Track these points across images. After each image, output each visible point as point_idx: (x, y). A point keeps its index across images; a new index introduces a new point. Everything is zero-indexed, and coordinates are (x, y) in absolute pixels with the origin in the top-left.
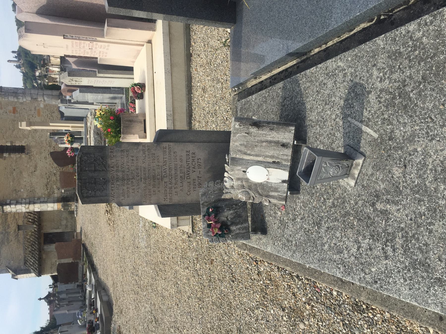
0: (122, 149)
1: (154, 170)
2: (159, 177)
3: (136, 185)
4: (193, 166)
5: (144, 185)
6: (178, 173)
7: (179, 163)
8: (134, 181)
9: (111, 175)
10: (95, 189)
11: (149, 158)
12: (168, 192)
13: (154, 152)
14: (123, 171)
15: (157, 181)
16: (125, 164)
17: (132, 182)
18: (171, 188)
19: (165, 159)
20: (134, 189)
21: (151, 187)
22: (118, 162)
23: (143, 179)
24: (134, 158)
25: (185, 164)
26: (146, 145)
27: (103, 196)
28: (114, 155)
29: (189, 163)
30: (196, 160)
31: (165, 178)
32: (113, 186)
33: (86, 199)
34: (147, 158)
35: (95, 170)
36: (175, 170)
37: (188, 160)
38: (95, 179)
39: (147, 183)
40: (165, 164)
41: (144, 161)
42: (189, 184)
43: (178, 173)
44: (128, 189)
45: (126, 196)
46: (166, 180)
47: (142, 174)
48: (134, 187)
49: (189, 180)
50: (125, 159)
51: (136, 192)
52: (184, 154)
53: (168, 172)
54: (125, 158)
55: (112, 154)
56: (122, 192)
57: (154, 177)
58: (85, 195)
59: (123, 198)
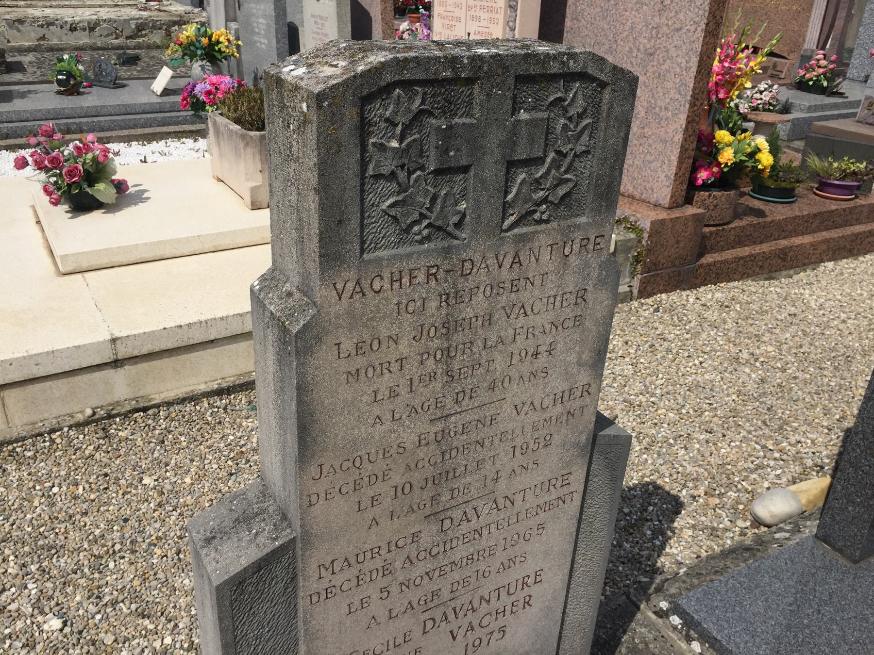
0: (589, 297)
1: (480, 463)
2: (445, 497)
3: (417, 402)
4: (475, 623)
5: (409, 438)
6: (456, 576)
7: (501, 556)
8: (437, 385)
9: (477, 258)
10: (410, 173)
11: (535, 429)
12: (369, 565)
13: (557, 439)
14: (489, 320)
15: (427, 494)
16: (522, 320)
17: (433, 377)
18: (386, 570)
19: (519, 498)
20: (393, 394)
21: (397, 479)
22: (538, 282)
23: (440, 426)
24: (543, 358)
25: (487, 588)
26: (588, 400)
27: (362, 227)
28: (572, 258)
29: (493, 600)
30: (501, 622)
31: (435, 528)
32: (421, 277)
33: (350, 115)
34: (534, 417)
35: (512, 165)
36: (470, 558)
37: (503, 593)
38: (465, 169)
39: (422, 453)
40: (501, 502)
41: (526, 408)
42: (400, 640)
43: (456, 576)
44: (395, 367)
45: (360, 362)
46: (429, 534)
47: (468, 417)
48: (403, 391)
49: (418, 631)
50: (542, 320)
51: (376, 410)
52: (530, 568)
53: (465, 527)
54: (550, 316)
55: (576, 247)
56: (384, 333)
57: (449, 474)
58: (378, 111)
59: (348, 345)
